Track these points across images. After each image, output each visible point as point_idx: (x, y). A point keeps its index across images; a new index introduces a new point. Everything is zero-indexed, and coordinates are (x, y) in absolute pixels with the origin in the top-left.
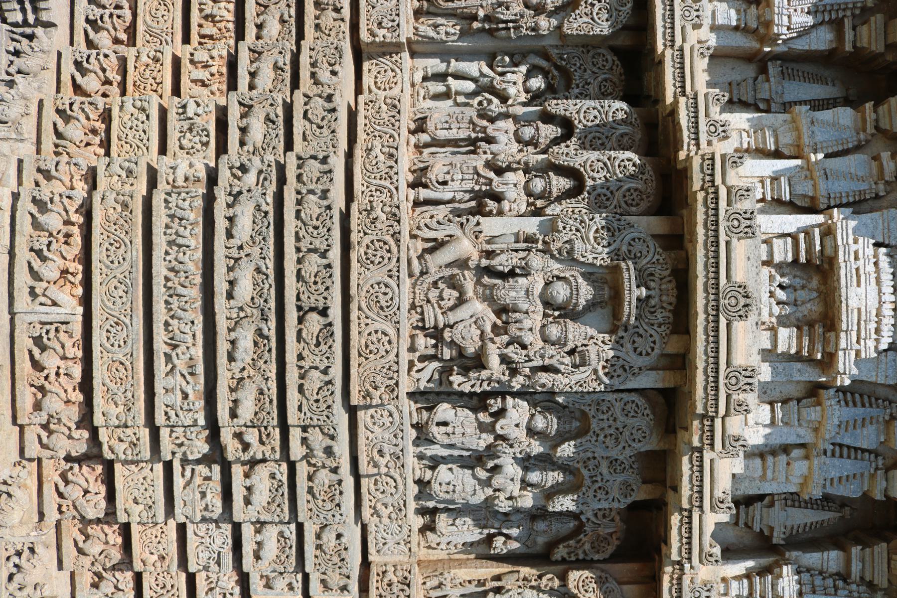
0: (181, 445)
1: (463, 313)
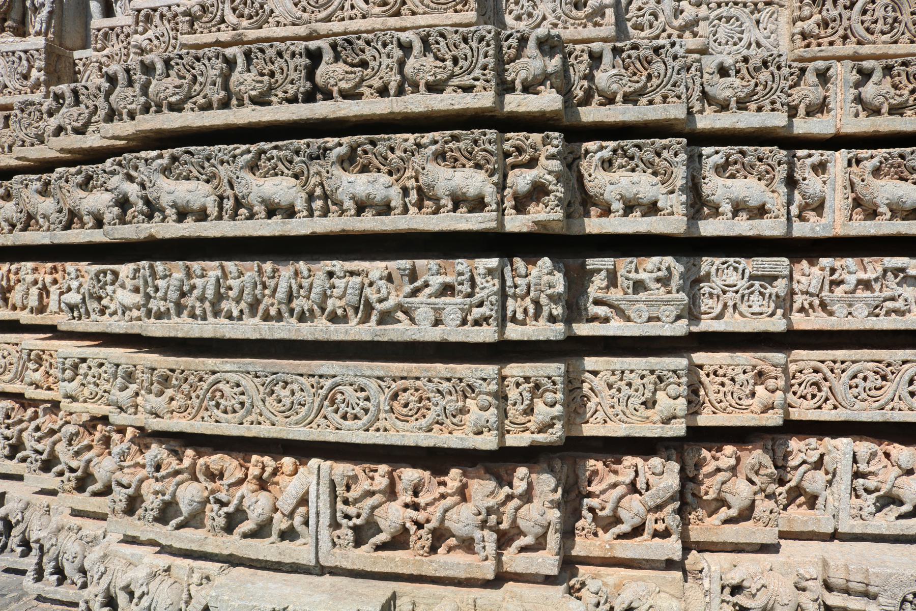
0: (537, 303)
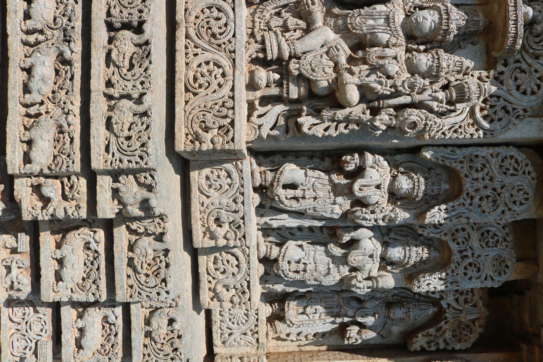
1: (313, 41)
